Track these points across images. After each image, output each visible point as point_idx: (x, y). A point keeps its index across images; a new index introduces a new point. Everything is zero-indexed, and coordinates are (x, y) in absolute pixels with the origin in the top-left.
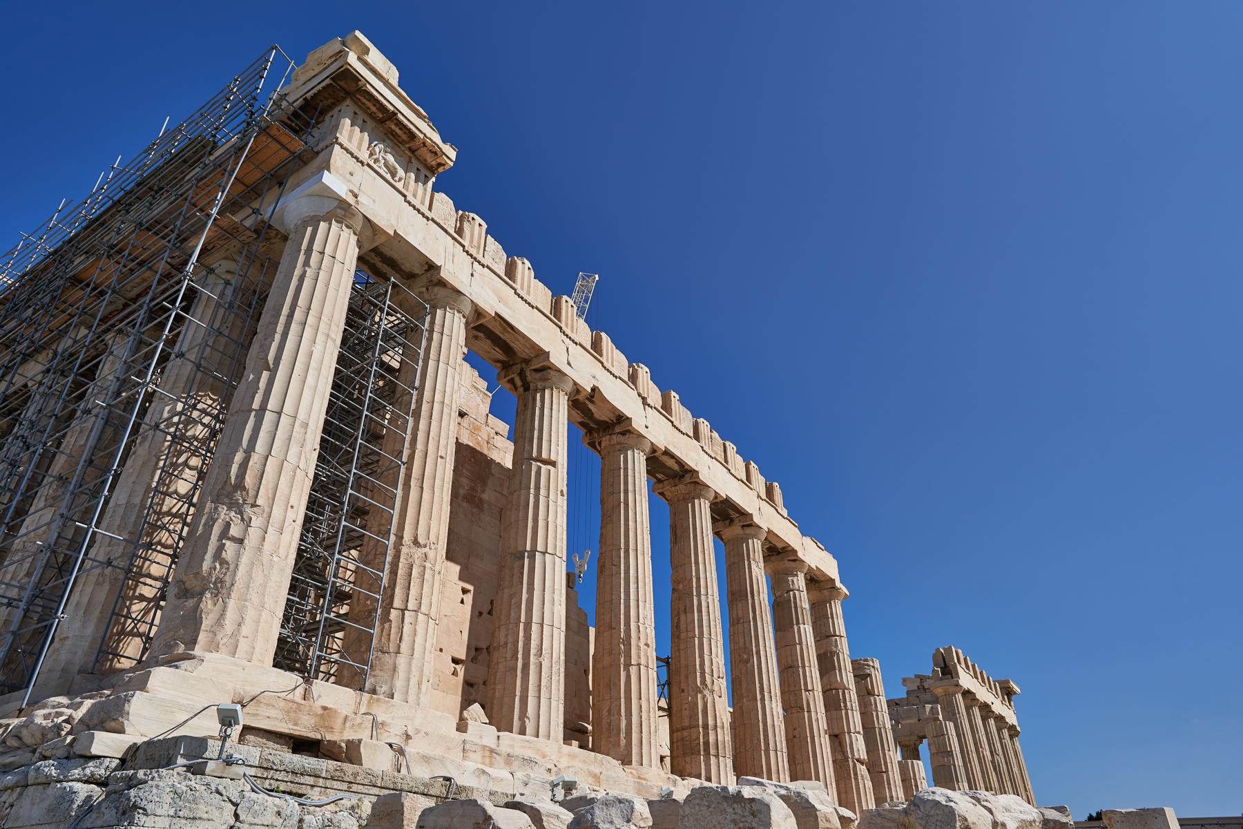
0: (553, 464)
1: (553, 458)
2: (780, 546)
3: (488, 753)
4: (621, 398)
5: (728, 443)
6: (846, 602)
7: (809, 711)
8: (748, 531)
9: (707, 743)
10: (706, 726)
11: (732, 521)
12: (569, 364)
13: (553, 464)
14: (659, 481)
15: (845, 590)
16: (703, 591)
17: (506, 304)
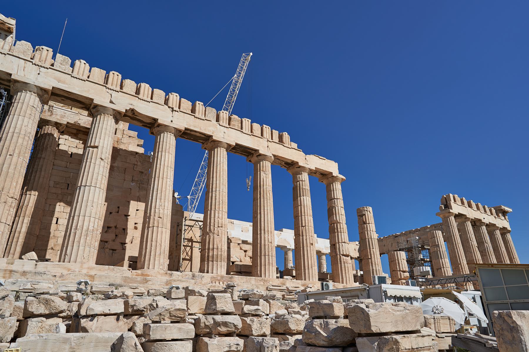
0: (97, 147)
1: (96, 145)
2: (290, 162)
3: (9, 272)
4: (146, 109)
5: (243, 119)
6: (343, 183)
7: (303, 236)
8: (260, 158)
9: (208, 256)
10: (209, 249)
11: (253, 154)
12: (111, 102)
13: (97, 147)
14: (203, 143)
15: (341, 176)
16: (214, 190)
17: (64, 82)
